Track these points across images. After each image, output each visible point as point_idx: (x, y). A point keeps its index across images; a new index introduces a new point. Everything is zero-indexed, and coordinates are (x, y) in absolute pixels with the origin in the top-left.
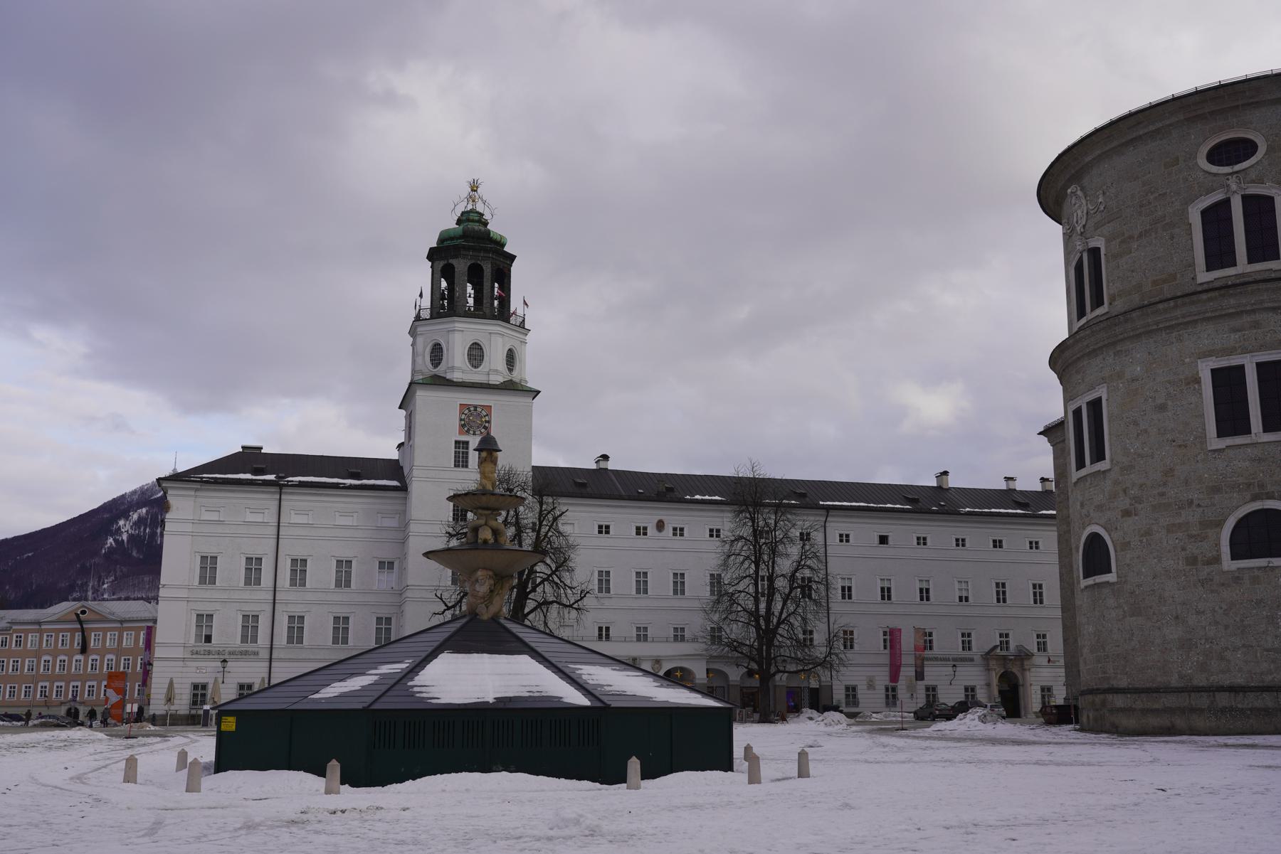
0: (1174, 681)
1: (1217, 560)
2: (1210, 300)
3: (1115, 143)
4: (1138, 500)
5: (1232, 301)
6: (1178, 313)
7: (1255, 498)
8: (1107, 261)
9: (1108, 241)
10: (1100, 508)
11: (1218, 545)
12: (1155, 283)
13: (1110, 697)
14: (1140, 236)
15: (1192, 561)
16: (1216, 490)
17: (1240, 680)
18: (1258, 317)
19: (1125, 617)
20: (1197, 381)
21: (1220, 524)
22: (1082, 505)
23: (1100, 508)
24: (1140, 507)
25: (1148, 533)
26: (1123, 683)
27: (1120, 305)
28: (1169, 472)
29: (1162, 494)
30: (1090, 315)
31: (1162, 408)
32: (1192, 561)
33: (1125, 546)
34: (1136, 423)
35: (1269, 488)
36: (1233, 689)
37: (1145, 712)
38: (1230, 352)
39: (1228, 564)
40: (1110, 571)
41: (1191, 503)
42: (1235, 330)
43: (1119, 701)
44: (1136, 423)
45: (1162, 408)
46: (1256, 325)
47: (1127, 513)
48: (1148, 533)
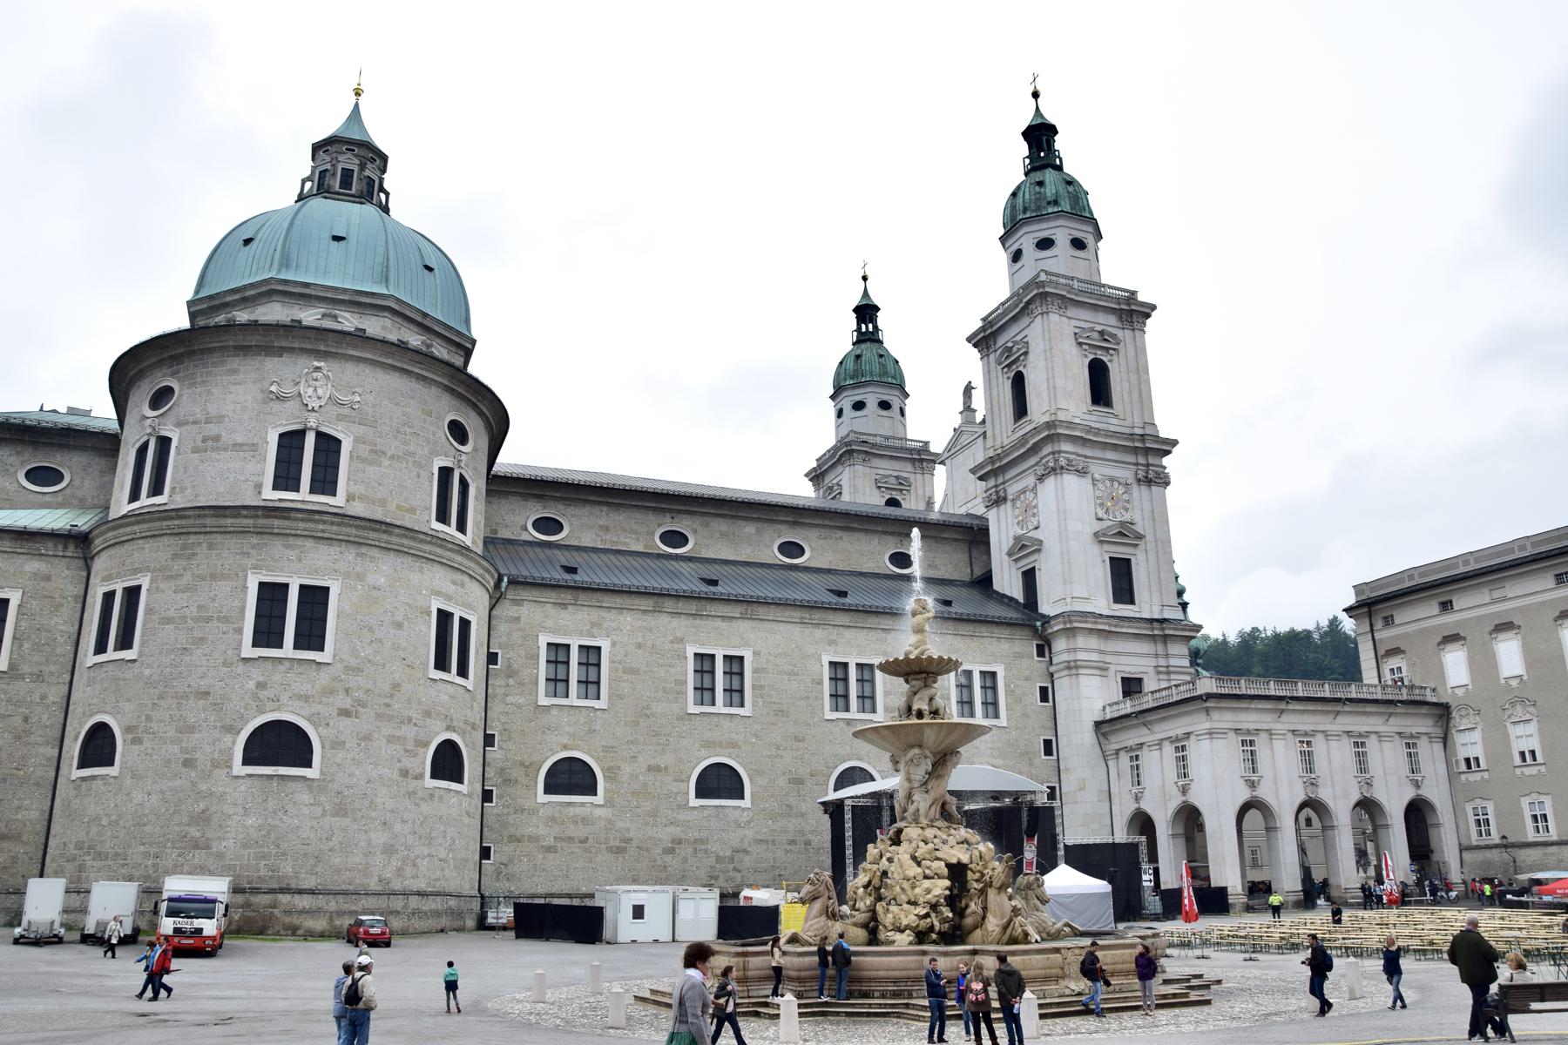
0: (373, 885)
1: (420, 777)
2: (450, 550)
3: (390, 361)
4: (364, 705)
5: (459, 558)
6: (428, 547)
7: (448, 728)
8: (351, 458)
9: (356, 440)
10: (305, 698)
12: (398, 507)
13: (284, 899)
14: (392, 457)
15: (405, 773)
17: (421, 885)
18: (466, 579)
19: (323, 815)
20: (429, 614)
21: (426, 745)
22: (261, 686)
23: (305, 698)
24: (362, 710)
25: (368, 738)
26: (310, 883)
27: (358, 509)
28: (396, 686)
29: (388, 705)
30: (303, 495)
31: (399, 626)
32: (405, 773)
33: (337, 744)
34: (371, 629)
35: (455, 723)
36: (420, 894)
37: (341, 913)
38: (449, 598)
39: (430, 783)
40: (309, 765)
42: (454, 583)
43: (304, 902)
44: (371, 629)
45: (399, 626)
46: (463, 585)
47: (345, 713)
48: (368, 738)
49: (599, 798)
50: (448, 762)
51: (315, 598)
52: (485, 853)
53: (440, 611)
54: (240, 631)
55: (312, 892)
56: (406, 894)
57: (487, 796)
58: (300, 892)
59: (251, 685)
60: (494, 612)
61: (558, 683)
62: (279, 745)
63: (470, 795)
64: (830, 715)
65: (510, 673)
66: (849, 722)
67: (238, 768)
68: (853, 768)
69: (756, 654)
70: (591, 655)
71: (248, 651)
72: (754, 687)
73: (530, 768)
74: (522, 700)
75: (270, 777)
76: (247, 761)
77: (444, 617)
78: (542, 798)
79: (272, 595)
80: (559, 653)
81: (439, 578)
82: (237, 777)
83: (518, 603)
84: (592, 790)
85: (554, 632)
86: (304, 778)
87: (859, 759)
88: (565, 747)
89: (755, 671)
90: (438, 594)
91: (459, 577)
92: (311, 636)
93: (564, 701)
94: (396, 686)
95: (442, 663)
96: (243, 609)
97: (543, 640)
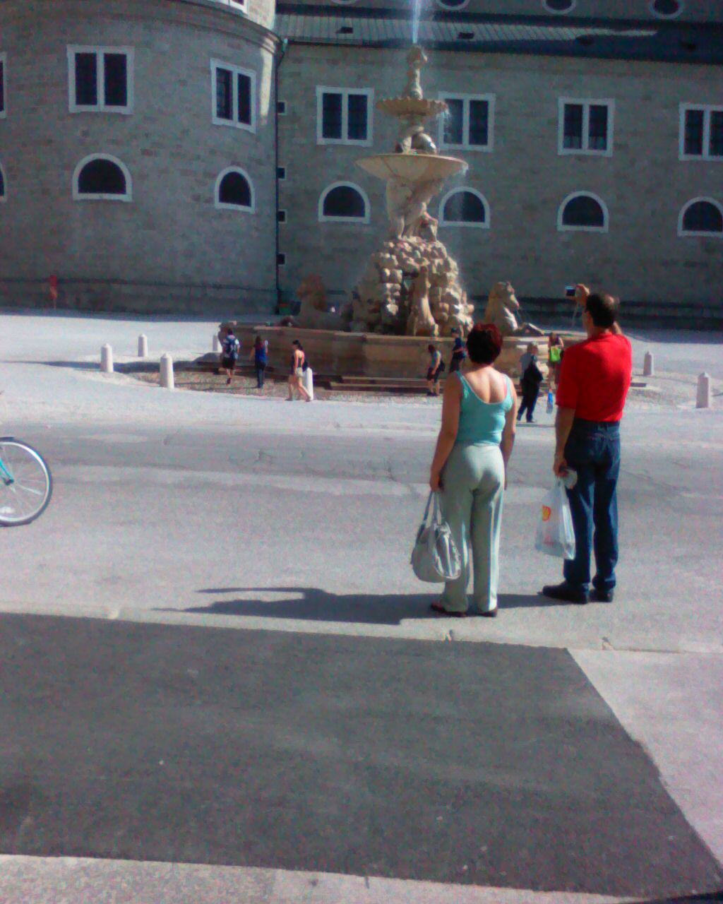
1: (210, 200)
7: (233, 163)
11: (212, 190)
13: (116, 286)
15: (197, 198)
16: (213, 152)
18: (243, 43)
20: (209, 72)
21: (214, 176)
22: (85, 134)
29: (179, 146)
31: (183, 83)
32: (197, 198)
41: (199, 157)
43: (127, 290)
45: (183, 83)
46: (239, 47)
47: (146, 152)
49: (366, 219)
50: (234, 190)
51: (116, 65)
52: (280, 259)
53: (219, 70)
54: (66, 92)
55: (134, 282)
56: (204, 286)
57: (280, 216)
58: (126, 283)
59: (78, 133)
60: (281, 69)
61: (331, 129)
62: (102, 177)
63: (257, 215)
64: (562, 151)
65: (294, 118)
66: (581, 158)
67: (77, 195)
68: (574, 200)
69: (499, 99)
70: (358, 103)
71: (73, 107)
72: (496, 127)
73: (313, 196)
74: (304, 141)
75: (98, 201)
76: (83, 189)
77: (224, 76)
78: (322, 218)
79: (85, 64)
80: (332, 102)
81: (216, 42)
82: (77, 202)
83: (299, 61)
84: (360, 213)
85: (328, 84)
86: (120, 202)
87: (587, 189)
88: (340, 178)
89: (498, 113)
90: (216, 56)
91: (237, 41)
92: (116, 94)
93: (336, 141)
94: (185, 132)
95: (225, 112)
96: (66, 76)
97: (320, 90)
